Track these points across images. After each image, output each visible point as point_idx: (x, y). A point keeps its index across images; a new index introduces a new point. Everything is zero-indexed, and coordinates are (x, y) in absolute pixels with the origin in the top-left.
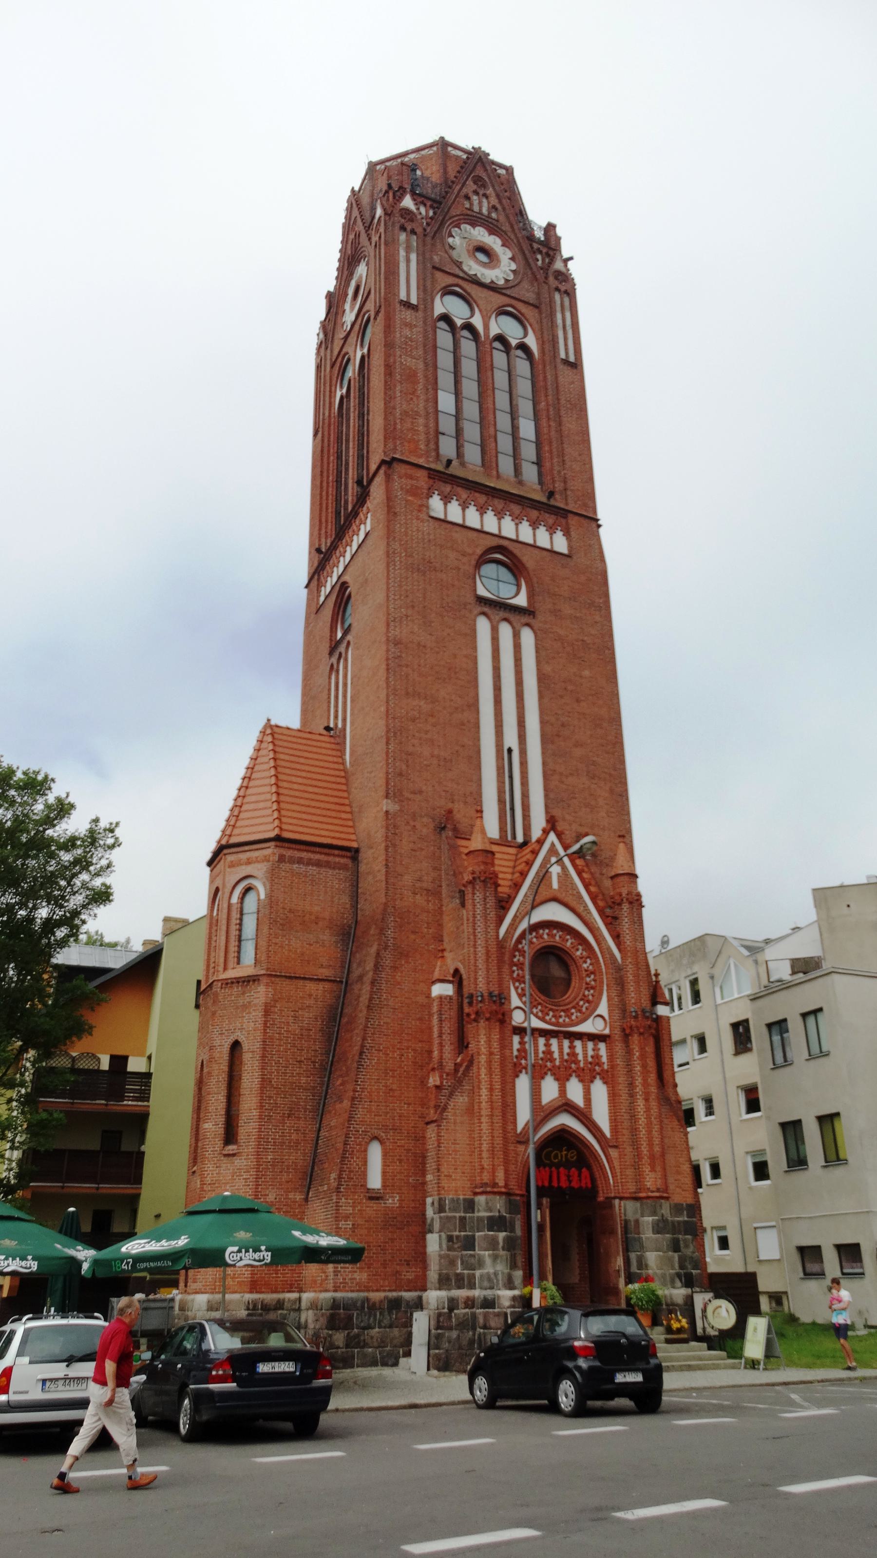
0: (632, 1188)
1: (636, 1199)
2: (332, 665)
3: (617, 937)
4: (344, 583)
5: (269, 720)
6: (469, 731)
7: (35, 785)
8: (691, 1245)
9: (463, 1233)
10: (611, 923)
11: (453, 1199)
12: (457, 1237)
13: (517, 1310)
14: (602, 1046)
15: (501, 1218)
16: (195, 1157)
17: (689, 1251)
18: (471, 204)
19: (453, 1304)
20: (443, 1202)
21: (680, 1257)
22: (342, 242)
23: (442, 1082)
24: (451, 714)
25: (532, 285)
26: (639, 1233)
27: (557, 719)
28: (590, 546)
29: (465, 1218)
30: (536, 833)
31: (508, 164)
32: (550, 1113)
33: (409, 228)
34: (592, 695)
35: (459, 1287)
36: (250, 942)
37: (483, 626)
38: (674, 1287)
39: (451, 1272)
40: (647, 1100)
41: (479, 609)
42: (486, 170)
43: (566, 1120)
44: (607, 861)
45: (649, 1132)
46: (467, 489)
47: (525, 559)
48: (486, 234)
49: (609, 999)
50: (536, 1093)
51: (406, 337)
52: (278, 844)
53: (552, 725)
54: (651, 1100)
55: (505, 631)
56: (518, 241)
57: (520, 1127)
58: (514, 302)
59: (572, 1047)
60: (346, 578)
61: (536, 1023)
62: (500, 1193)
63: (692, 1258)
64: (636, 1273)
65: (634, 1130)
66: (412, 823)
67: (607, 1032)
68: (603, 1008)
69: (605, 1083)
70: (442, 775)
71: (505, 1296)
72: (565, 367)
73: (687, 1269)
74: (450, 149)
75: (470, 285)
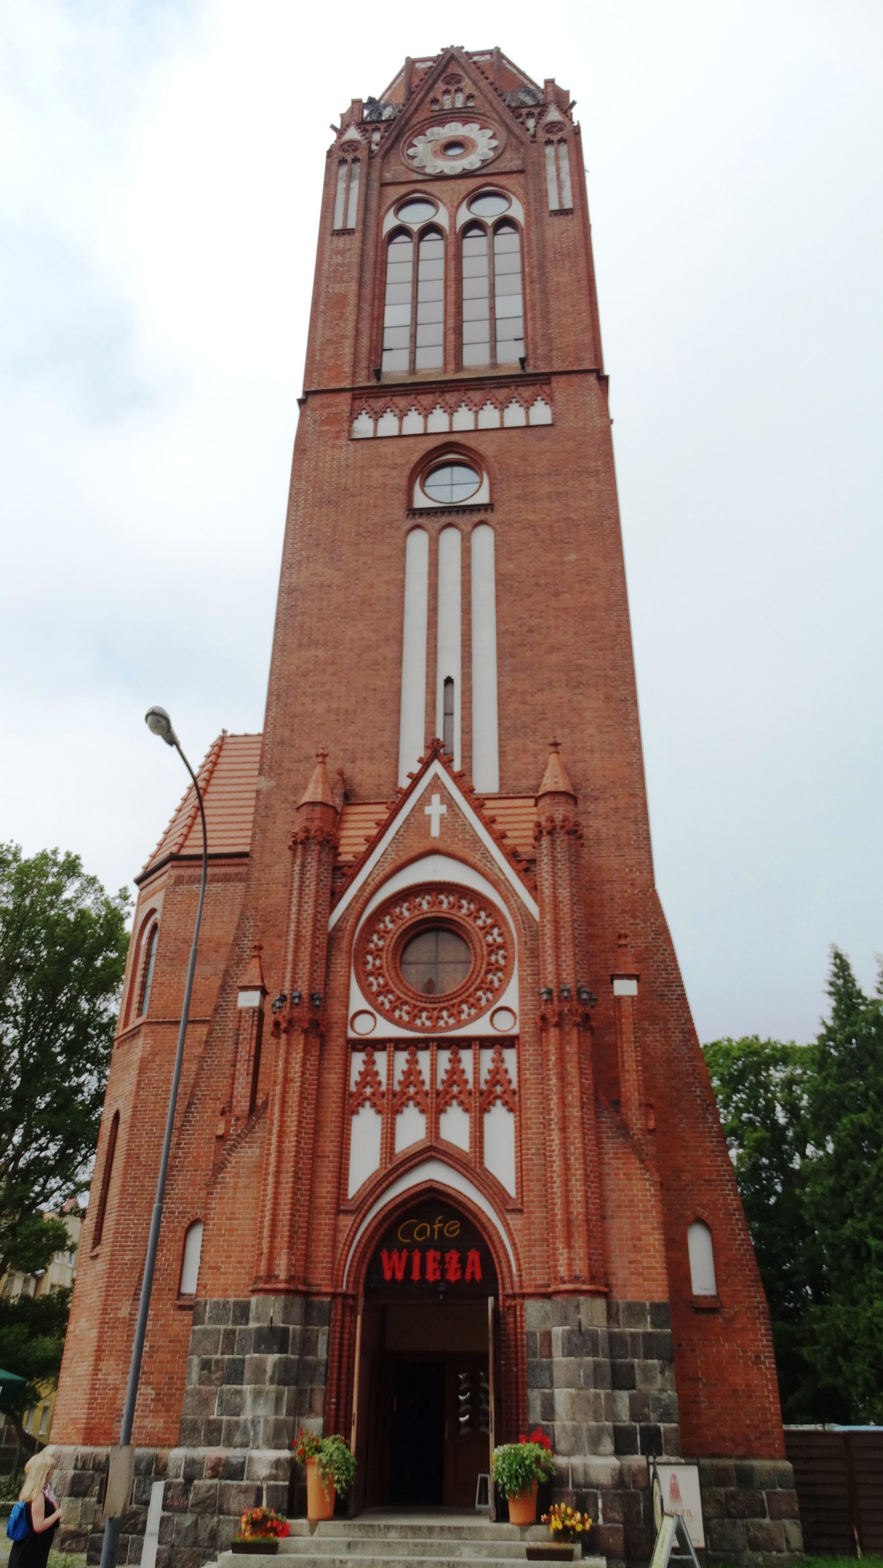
0: (540, 1278)
1: (547, 1296)
3: (534, 889)
6: (385, 669)
8: (659, 1377)
9: (227, 1357)
10: (527, 870)
11: (217, 1303)
12: (217, 1362)
13: (281, 1483)
14: (510, 1056)
15: (272, 1329)
17: (653, 1389)
19: (192, 1470)
20: (200, 1308)
21: (632, 1398)
23: (227, 1131)
24: (359, 656)
25: (517, 150)
26: (550, 1356)
27: (520, 626)
28: (584, 403)
29: (233, 1332)
31: (490, 47)
32: (402, 1164)
33: (349, 160)
34: (579, 582)
35: (210, 1444)
37: (418, 543)
38: (595, 1453)
39: (201, 1419)
40: (563, 1130)
41: (411, 523)
42: (460, 64)
44: (596, 793)
45: (566, 1182)
46: (406, 395)
47: (482, 449)
48: (459, 125)
49: (521, 980)
51: (337, 264)
52: (174, 863)
53: (513, 634)
54: (571, 1129)
56: (498, 113)
58: (489, 179)
61: (385, 1029)
62: (276, 1292)
63: (659, 1400)
64: (536, 1426)
65: (546, 1183)
66: (292, 798)
67: (515, 1031)
68: (511, 997)
69: (511, 1110)
70: (339, 732)
71: (264, 1459)
72: (556, 219)
73: (649, 1420)
74: (417, 65)
75: (431, 184)
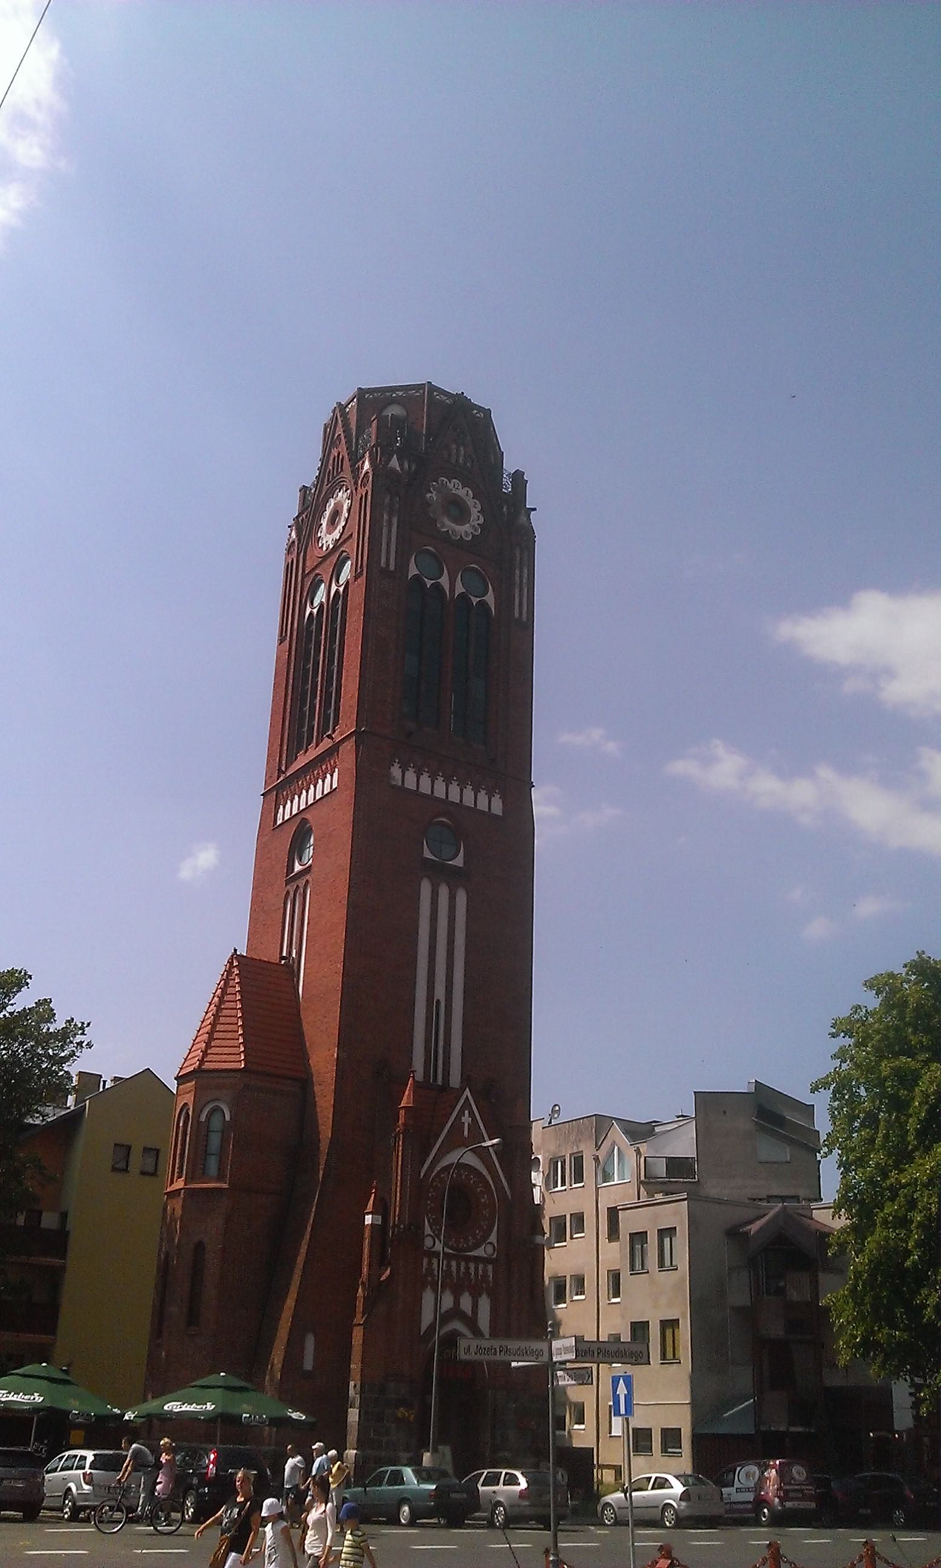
2: (288, 892)
4: (304, 821)
5: (235, 950)
7: (16, 981)
16: (158, 1330)
18: (450, 455)
22: (322, 460)
30: (455, 1080)
36: (213, 1157)
37: (426, 888)
43: (457, 1325)
50: (437, 1302)
55: (444, 892)
57: (424, 1328)
59: (467, 1268)
60: (308, 816)
